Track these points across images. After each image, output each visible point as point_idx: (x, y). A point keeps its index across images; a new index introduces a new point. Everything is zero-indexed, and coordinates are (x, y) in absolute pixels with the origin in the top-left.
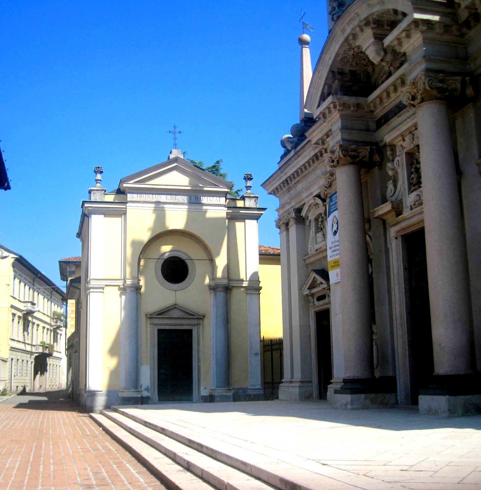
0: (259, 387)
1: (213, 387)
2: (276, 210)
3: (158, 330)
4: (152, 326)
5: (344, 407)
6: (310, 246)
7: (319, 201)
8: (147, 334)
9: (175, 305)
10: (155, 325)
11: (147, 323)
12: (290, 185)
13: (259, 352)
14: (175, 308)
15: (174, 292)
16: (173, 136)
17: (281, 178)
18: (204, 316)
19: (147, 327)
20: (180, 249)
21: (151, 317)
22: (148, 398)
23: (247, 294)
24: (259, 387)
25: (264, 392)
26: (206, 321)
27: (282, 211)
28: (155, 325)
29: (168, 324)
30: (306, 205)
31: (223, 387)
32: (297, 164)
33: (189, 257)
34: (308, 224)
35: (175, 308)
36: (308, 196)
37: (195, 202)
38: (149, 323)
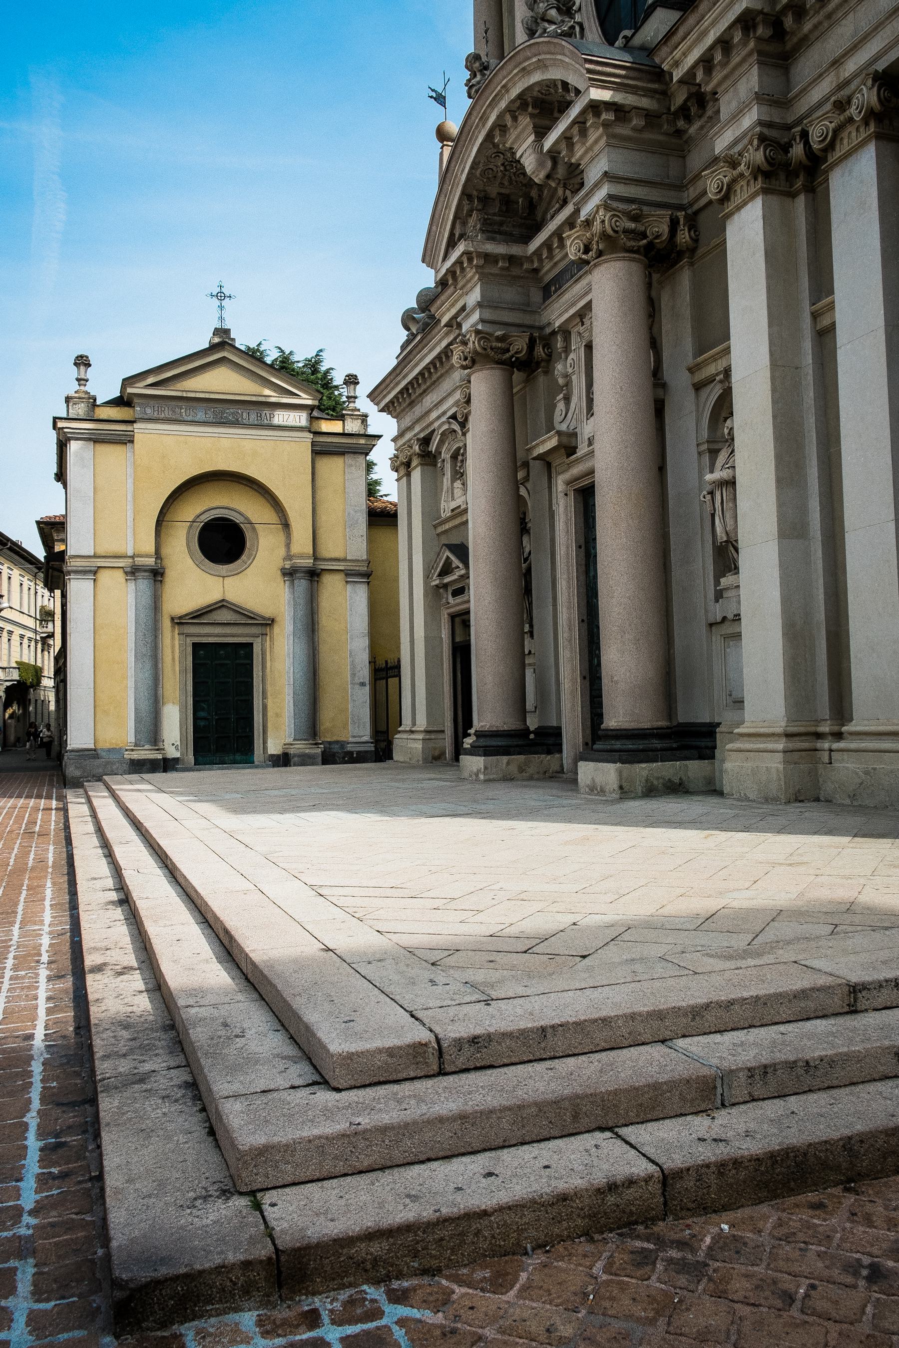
0: (367, 738)
1: (290, 740)
2: (392, 440)
4: (182, 637)
5: (474, 777)
6: (443, 504)
7: (456, 427)
9: (223, 600)
10: (188, 635)
11: (173, 631)
12: (413, 397)
14: (223, 606)
16: (218, 303)
17: (397, 384)
18: (273, 620)
19: (173, 638)
20: (231, 506)
21: (179, 622)
22: (176, 760)
23: (347, 582)
24: (367, 738)
25: (375, 747)
26: (276, 629)
27: (401, 442)
28: (188, 635)
29: (211, 635)
30: (436, 433)
31: (305, 740)
32: (421, 360)
33: (247, 518)
34: (439, 465)
36: (439, 417)
37: (256, 423)
38: (177, 632)
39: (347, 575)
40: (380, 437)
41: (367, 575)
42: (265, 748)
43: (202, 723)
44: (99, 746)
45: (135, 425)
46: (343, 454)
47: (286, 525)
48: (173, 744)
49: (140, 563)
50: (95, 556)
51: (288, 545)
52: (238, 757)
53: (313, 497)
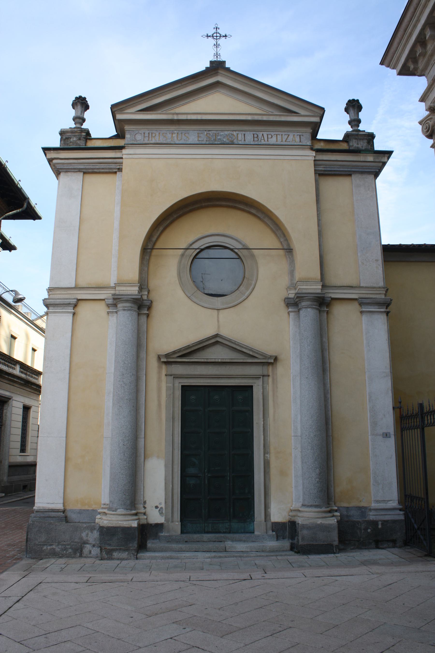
1: (297, 505)
3: (182, 386)
8: (159, 397)
9: (217, 336)
10: (176, 377)
11: (159, 373)
13: (391, 430)
14: (217, 343)
15: (216, 311)
16: (214, 42)
18: (276, 359)
21: (168, 360)
22: (159, 527)
23: (362, 312)
24: (394, 504)
25: (406, 515)
26: (280, 369)
28: (176, 377)
29: (202, 375)
31: (316, 506)
33: (244, 246)
35: (217, 343)
37: (252, 143)
38: (164, 372)
39: (361, 304)
40: (389, 153)
41: (387, 304)
42: (267, 515)
43: (192, 482)
44: (69, 507)
45: (124, 151)
46: (349, 174)
47: (289, 251)
48: (157, 507)
49: (122, 293)
50: (76, 288)
51: (292, 273)
52: (235, 525)
53: (319, 220)
